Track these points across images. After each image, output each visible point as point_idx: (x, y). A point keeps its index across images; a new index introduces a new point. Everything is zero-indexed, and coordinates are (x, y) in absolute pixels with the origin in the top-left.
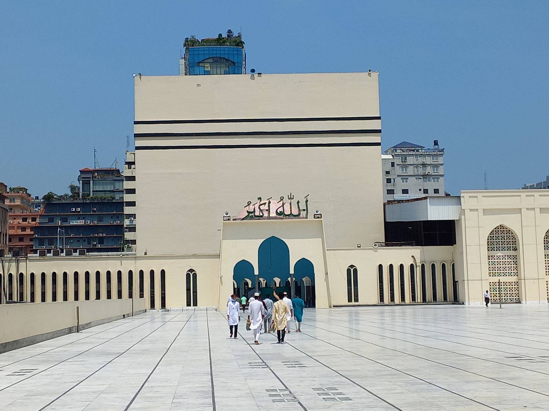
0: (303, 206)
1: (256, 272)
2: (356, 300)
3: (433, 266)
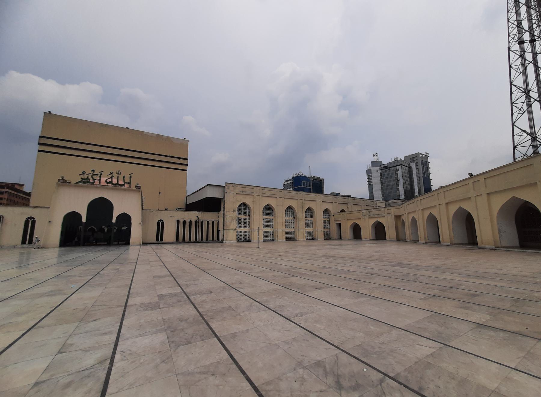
0: (127, 180)
1: (84, 220)
2: (162, 240)
3: (208, 222)
